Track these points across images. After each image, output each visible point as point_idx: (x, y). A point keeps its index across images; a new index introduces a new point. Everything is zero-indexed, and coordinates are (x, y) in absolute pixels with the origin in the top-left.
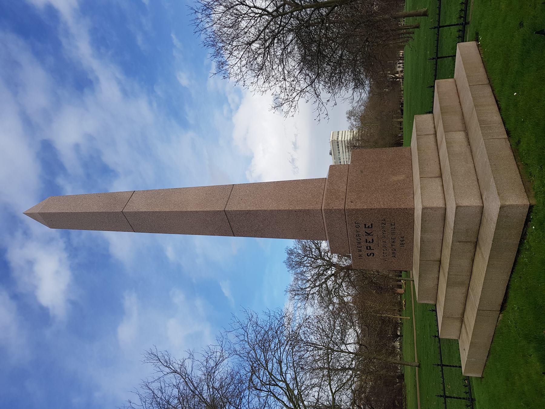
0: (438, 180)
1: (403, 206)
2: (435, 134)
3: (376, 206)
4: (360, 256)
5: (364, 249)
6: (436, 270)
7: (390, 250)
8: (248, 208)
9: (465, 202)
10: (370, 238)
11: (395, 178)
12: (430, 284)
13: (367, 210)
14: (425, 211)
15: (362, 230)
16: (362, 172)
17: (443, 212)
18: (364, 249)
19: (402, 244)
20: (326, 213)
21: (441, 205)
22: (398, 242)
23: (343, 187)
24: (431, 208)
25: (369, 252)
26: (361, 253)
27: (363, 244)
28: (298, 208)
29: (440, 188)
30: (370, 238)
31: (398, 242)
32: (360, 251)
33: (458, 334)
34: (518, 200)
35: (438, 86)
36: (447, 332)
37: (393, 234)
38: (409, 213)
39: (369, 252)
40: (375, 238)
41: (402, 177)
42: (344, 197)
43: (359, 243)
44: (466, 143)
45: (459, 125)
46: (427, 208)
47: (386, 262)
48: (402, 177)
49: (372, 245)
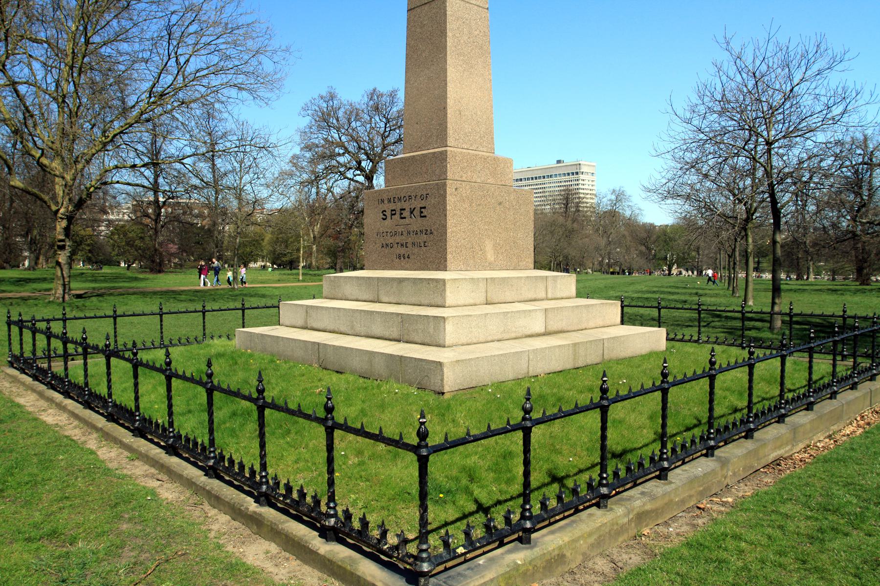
0: (482, 299)
1: (449, 256)
2: (547, 299)
3: (450, 222)
4: (383, 201)
5: (392, 206)
7: (391, 241)
8: (449, 34)
9: (449, 327)
10: (406, 214)
11: (489, 246)
12: (348, 290)
13: (445, 210)
14: (441, 283)
15: (417, 204)
16: (500, 204)
17: (439, 303)
18: (392, 206)
20: (441, 153)
21: (448, 303)
22: (402, 251)
23: (478, 177)
24: (444, 290)
25: (388, 214)
26: (386, 202)
27: (399, 206)
28: (449, 111)
29: (472, 301)
31: (402, 251)
32: (389, 201)
33: (288, 323)
34: (451, 381)
35: (612, 304)
36: (289, 309)
38: (442, 265)
39: (388, 214)
40: (407, 221)
41: (490, 256)
42: (464, 179)
44: (529, 333)
45: (554, 326)
46: (445, 285)
47: (375, 235)
48: (490, 256)
49: (397, 216)
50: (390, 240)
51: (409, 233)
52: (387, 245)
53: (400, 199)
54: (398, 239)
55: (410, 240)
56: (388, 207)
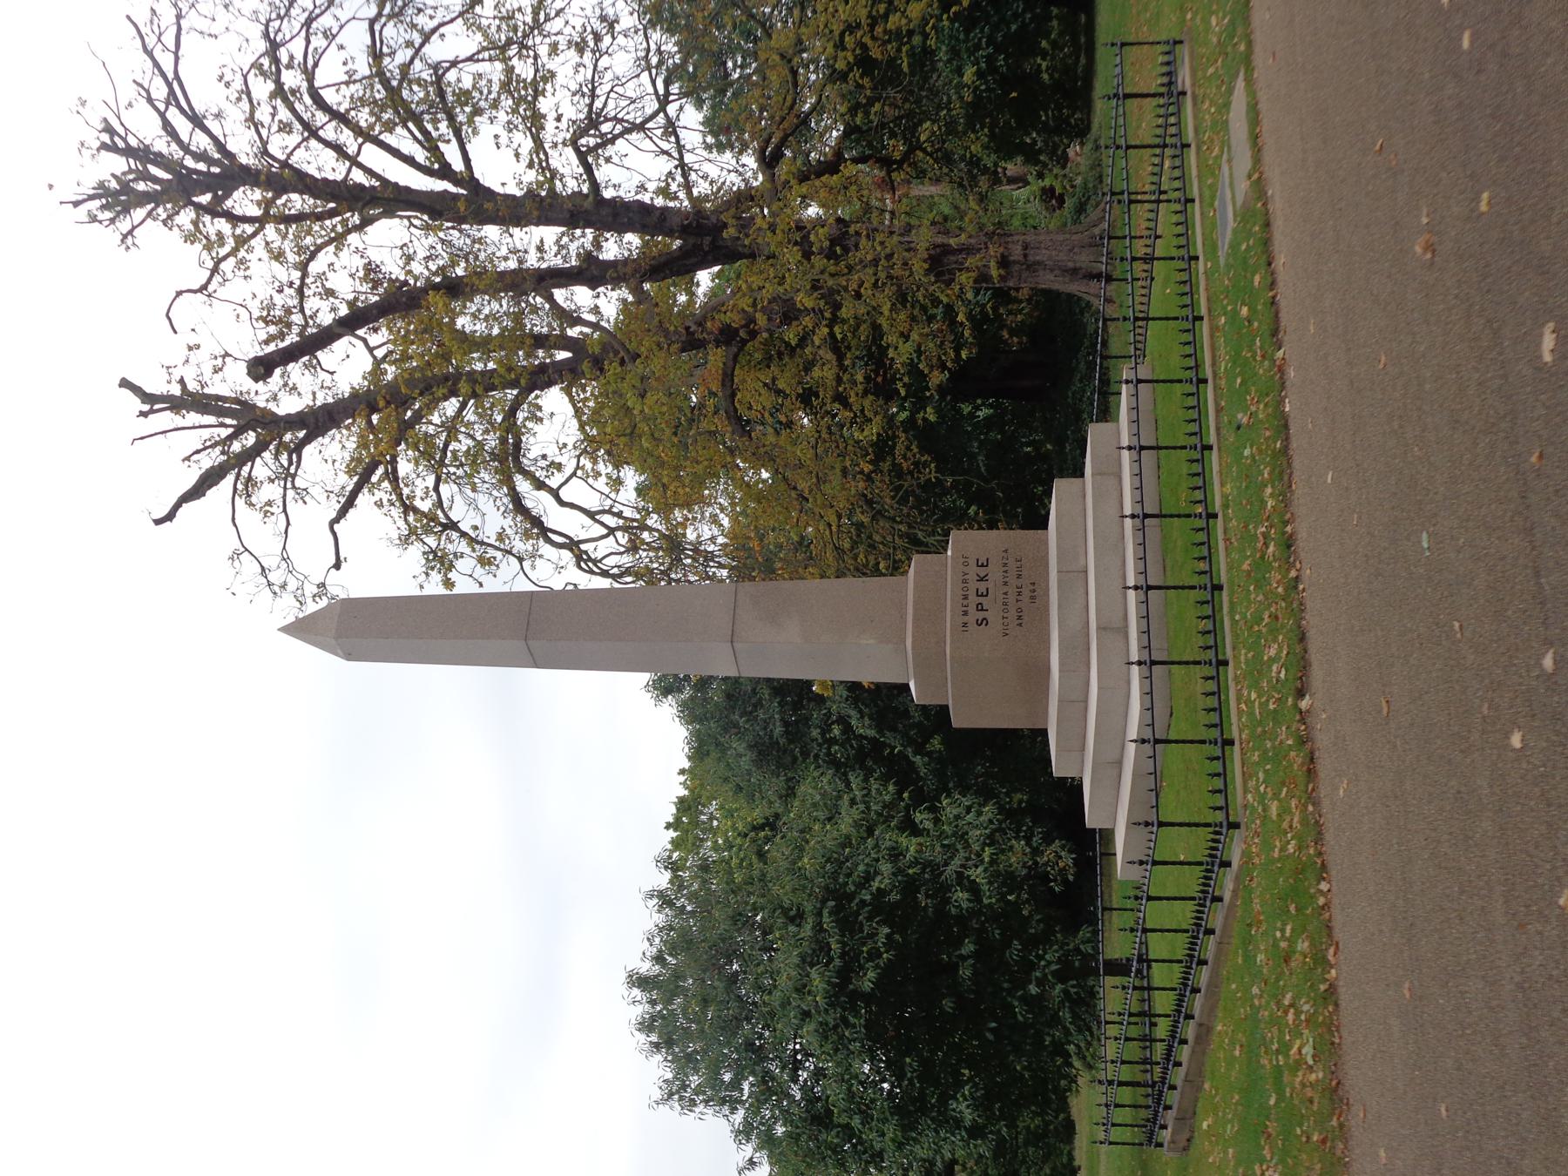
5: (972, 609)
6: (1082, 590)
10: (982, 587)
15: (973, 571)
18: (972, 609)
19: (1032, 598)
22: (1026, 592)
25: (981, 615)
26: (966, 619)
30: (982, 587)
31: (1026, 592)
32: (965, 613)
37: (1019, 576)
39: (981, 615)
40: (990, 585)
43: (966, 597)
50: (1013, 614)
51: (1006, 583)
52: (1020, 618)
53: (966, 597)
54: (1012, 598)
55: (1013, 581)
56: (974, 615)
